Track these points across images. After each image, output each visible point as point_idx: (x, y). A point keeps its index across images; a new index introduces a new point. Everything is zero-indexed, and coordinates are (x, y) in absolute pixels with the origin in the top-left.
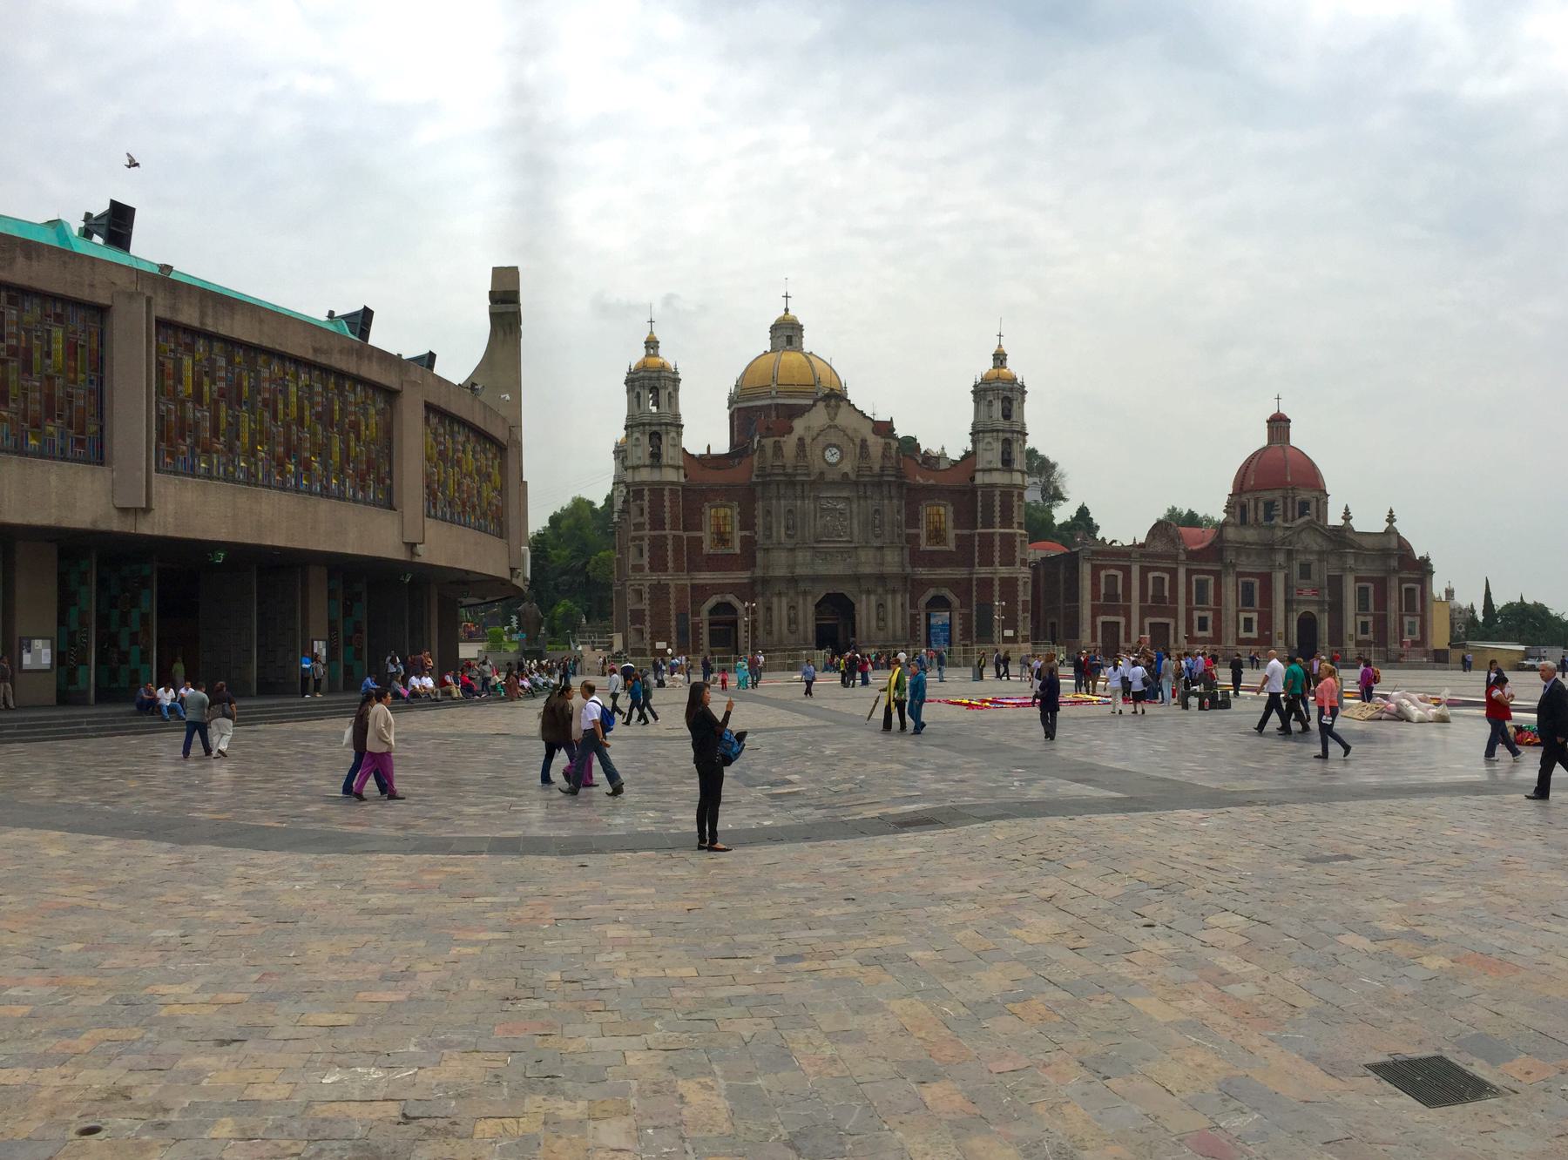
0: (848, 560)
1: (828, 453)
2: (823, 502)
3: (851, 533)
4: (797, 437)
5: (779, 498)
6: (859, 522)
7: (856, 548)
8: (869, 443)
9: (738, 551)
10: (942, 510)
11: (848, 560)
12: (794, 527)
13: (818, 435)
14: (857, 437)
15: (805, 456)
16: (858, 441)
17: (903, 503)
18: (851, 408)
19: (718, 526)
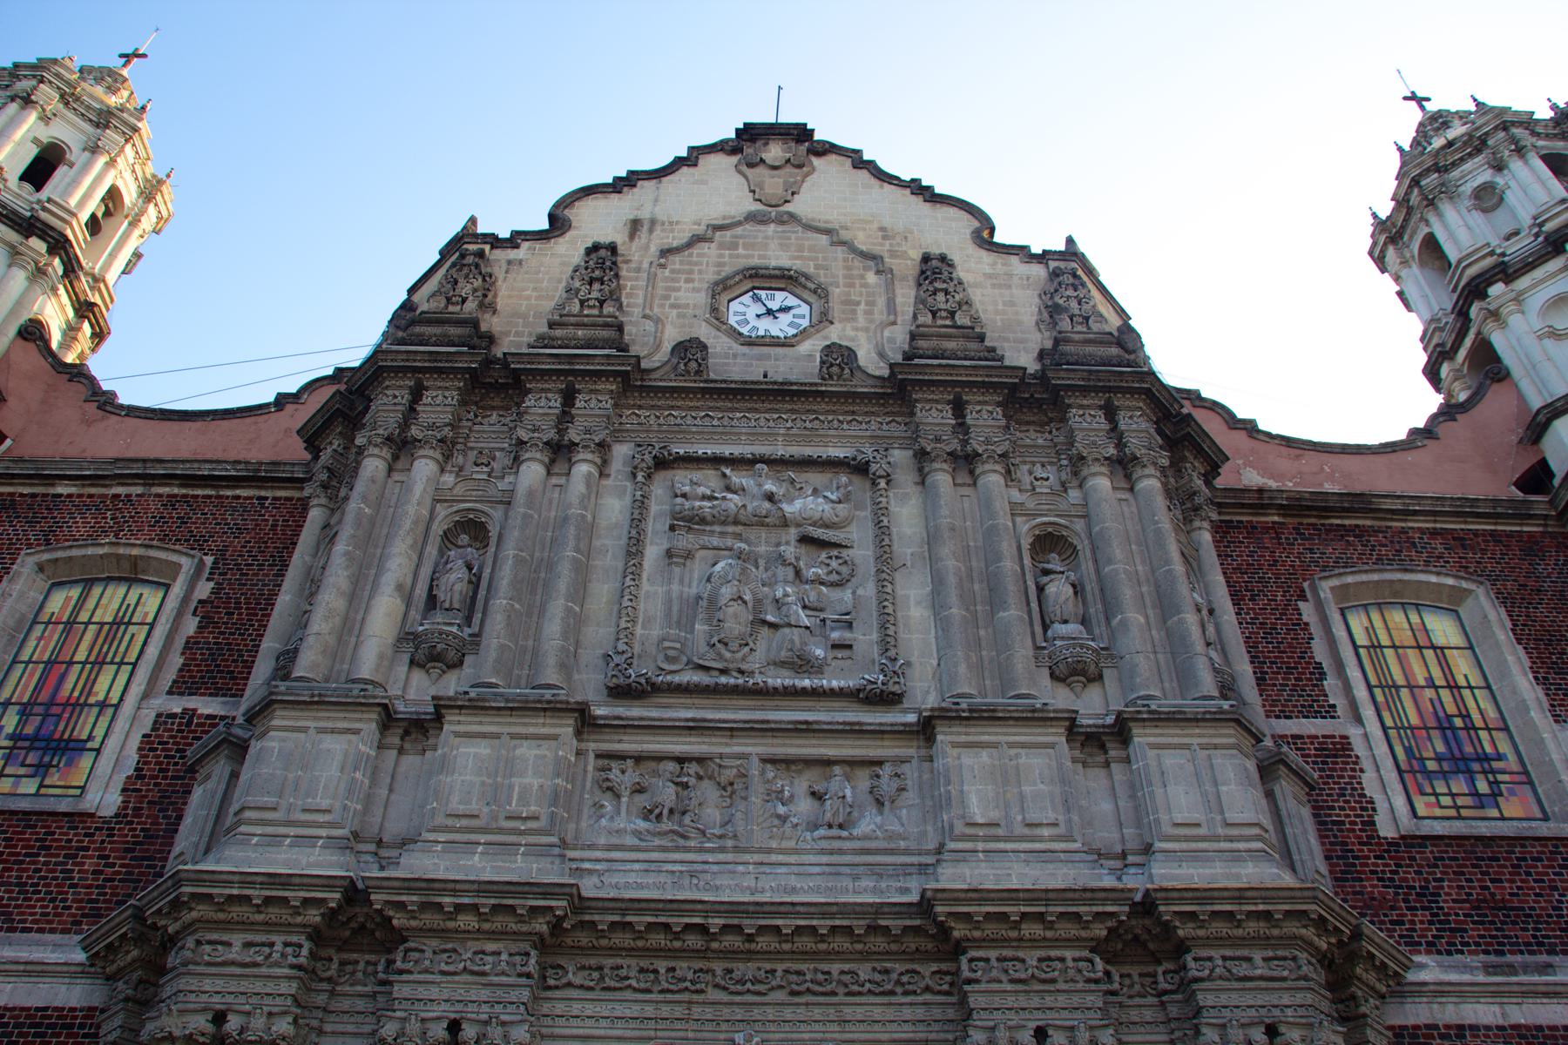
0: (868, 823)
1: (744, 312)
2: (682, 478)
3: (887, 643)
4: (589, 245)
5: (401, 447)
6: (937, 602)
7: (926, 729)
8: (961, 273)
9: (105, 798)
10: (1443, 629)
11: (868, 823)
12: (471, 607)
13: (697, 240)
14: (893, 254)
15: (614, 297)
16: (907, 264)
17: (1206, 537)
18: (864, 175)
19: (55, 666)
